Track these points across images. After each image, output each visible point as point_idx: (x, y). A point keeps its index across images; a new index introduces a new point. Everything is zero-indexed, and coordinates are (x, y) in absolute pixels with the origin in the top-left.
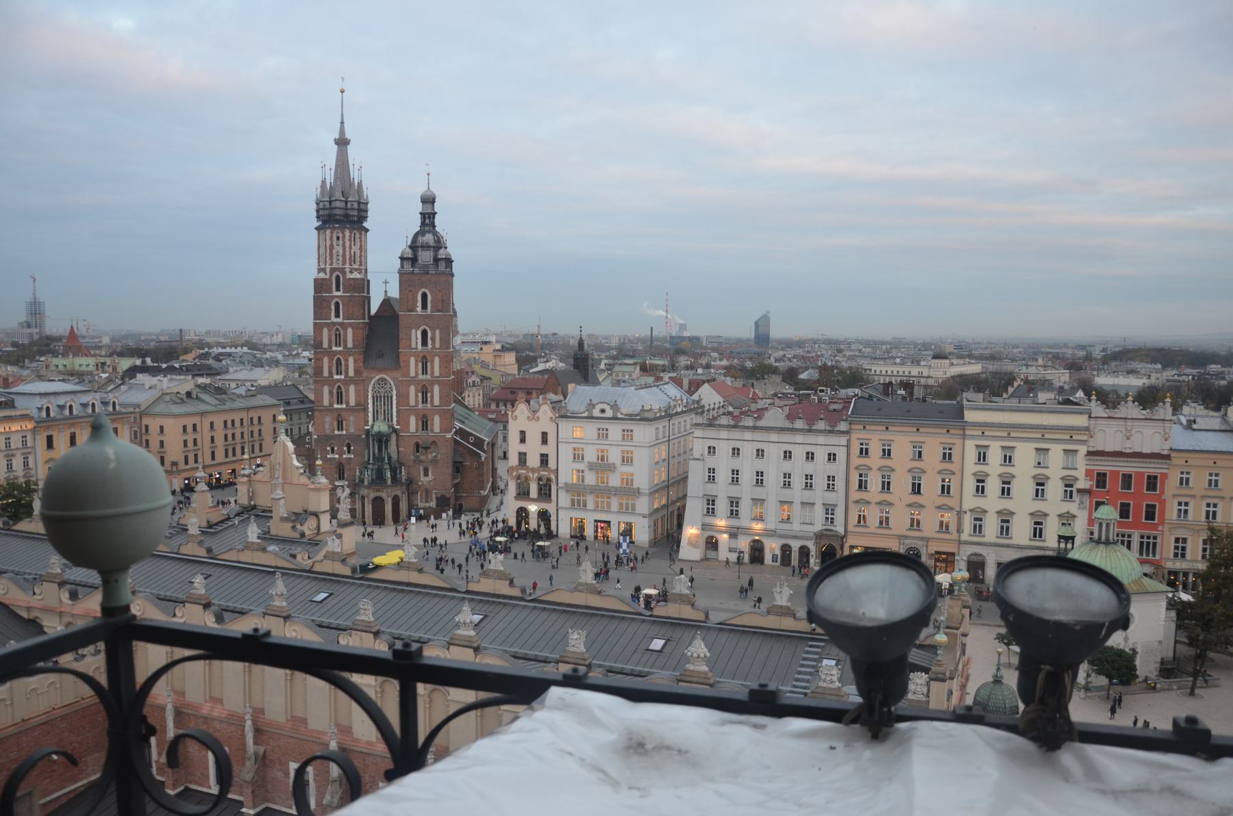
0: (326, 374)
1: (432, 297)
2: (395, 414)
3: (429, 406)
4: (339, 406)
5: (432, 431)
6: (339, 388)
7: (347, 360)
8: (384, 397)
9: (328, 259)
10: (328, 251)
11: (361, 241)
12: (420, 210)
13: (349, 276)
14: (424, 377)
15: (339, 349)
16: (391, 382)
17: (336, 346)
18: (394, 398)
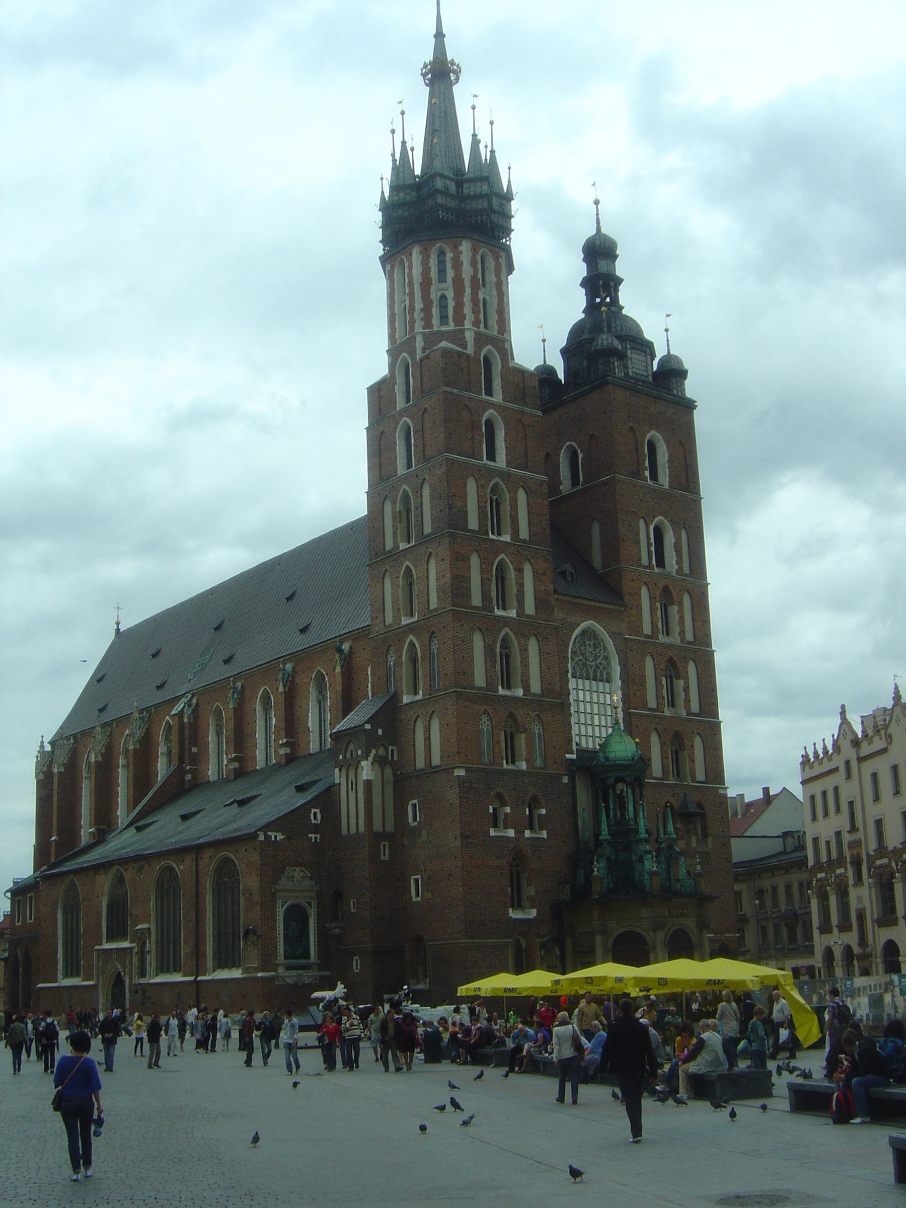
0: (476, 600)
1: (670, 455)
3: (684, 713)
4: (507, 693)
7: (520, 570)
9: (467, 309)
10: (468, 290)
17: (493, 533)
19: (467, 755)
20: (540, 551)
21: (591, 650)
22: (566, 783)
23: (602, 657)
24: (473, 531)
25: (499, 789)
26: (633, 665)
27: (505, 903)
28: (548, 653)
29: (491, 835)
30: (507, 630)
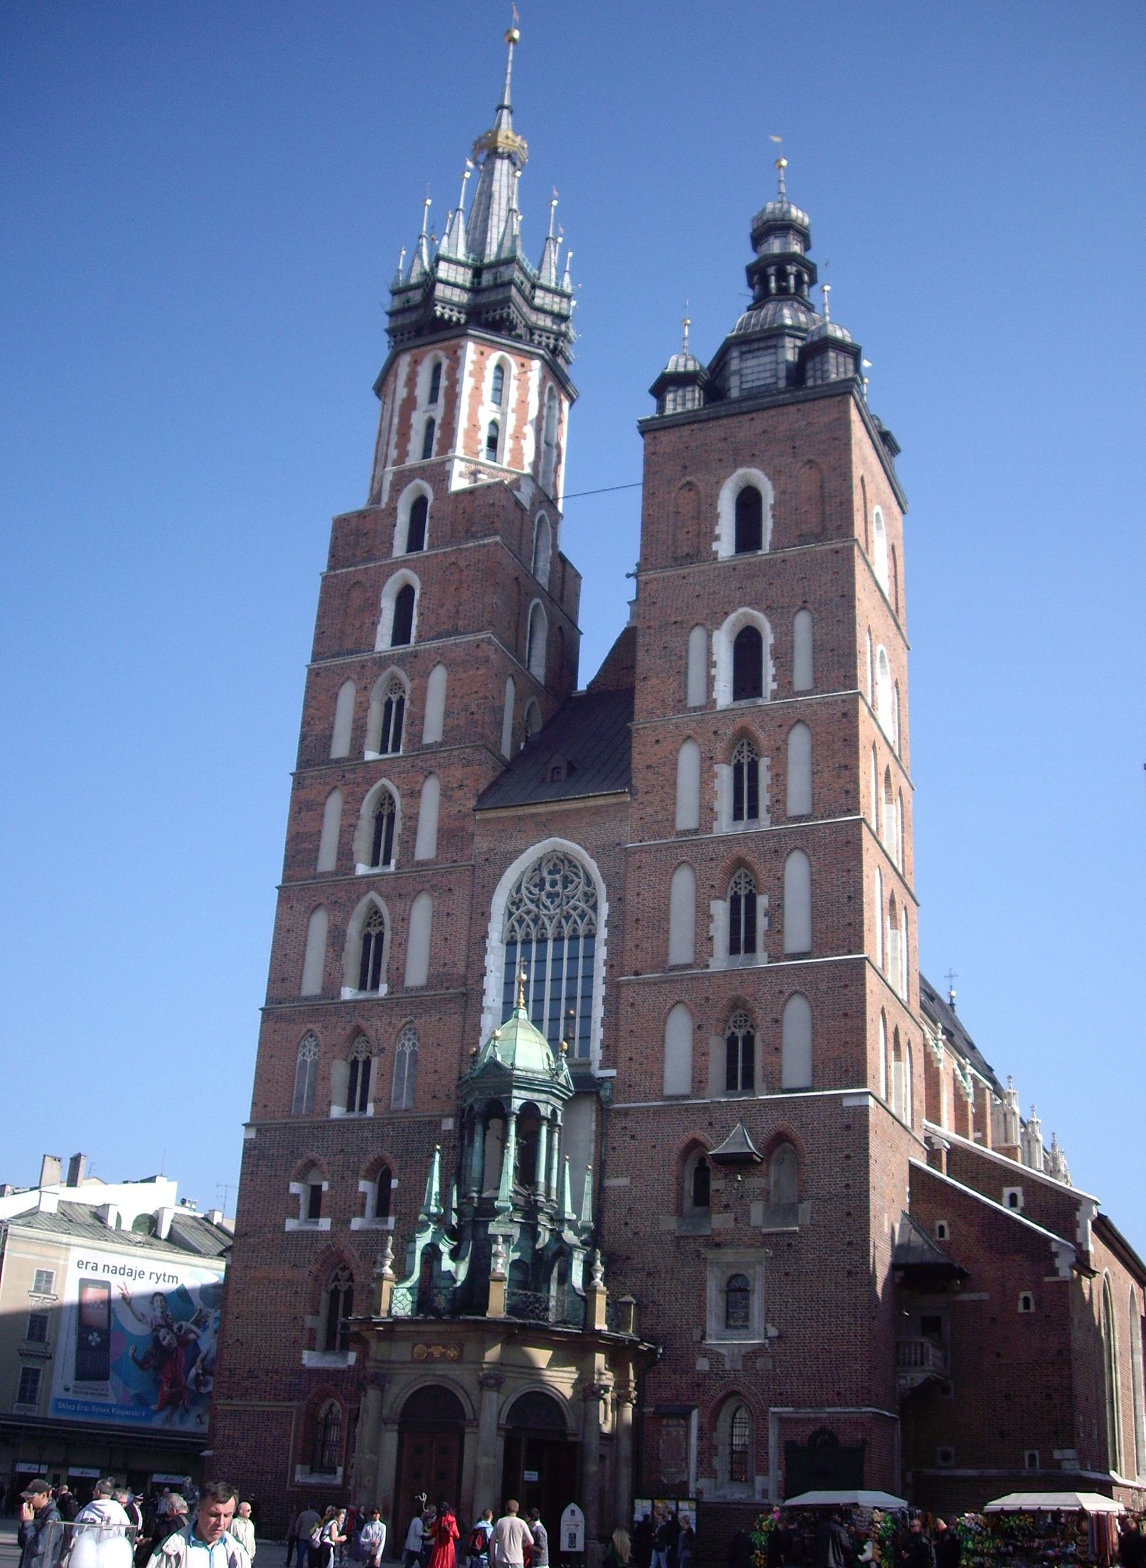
0: (327, 861)
1: (781, 493)
2: (598, 1011)
4: (362, 996)
5: (774, 1084)
6: (374, 915)
7: (414, 795)
8: (559, 939)
10: (396, 420)
11: (524, 387)
12: (752, 258)
13: (458, 483)
14: (741, 827)
15: (390, 755)
16: (593, 866)
17: (383, 750)
18: (602, 933)
19: (266, 1106)
20: (456, 753)
21: (559, 888)
22: (449, 1131)
23: (579, 893)
24: (338, 761)
25: (313, 1155)
26: (638, 894)
27: (295, 1342)
28: (448, 914)
29: (287, 1229)
30: (373, 895)
